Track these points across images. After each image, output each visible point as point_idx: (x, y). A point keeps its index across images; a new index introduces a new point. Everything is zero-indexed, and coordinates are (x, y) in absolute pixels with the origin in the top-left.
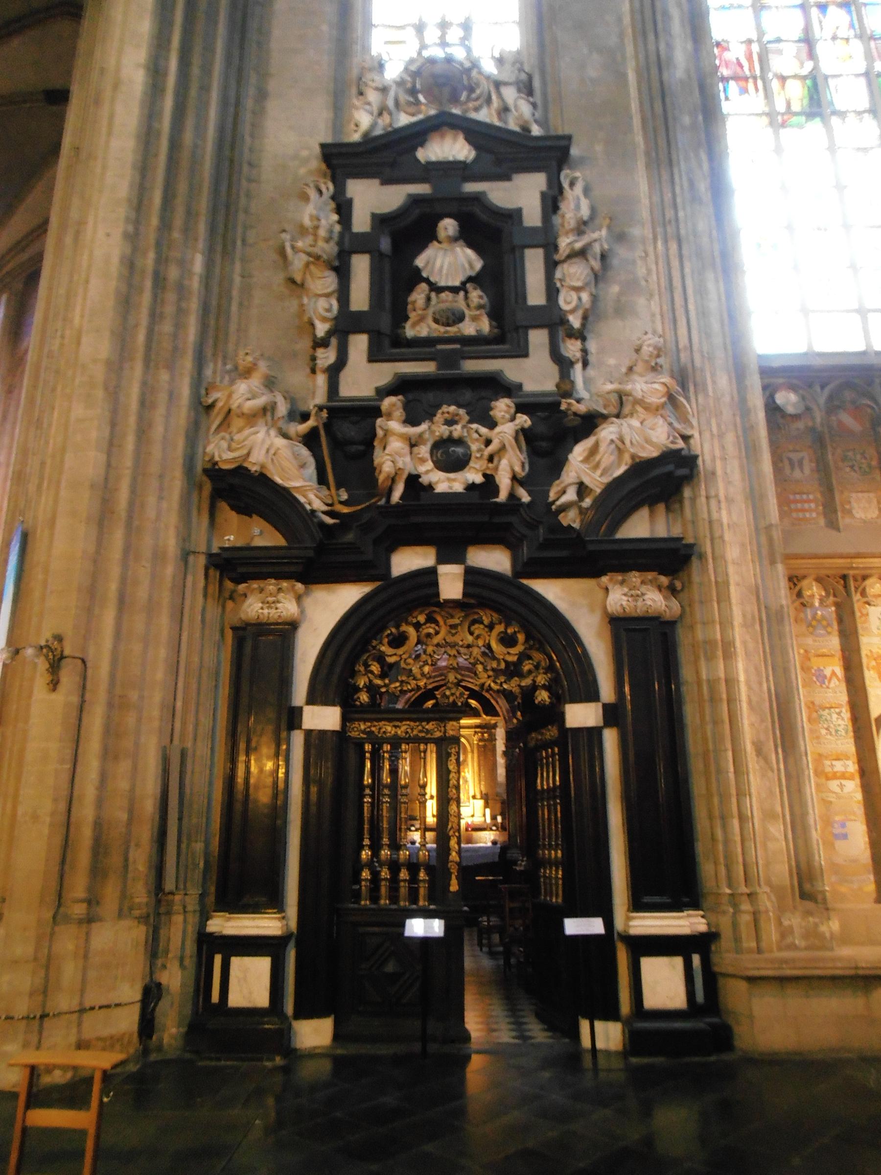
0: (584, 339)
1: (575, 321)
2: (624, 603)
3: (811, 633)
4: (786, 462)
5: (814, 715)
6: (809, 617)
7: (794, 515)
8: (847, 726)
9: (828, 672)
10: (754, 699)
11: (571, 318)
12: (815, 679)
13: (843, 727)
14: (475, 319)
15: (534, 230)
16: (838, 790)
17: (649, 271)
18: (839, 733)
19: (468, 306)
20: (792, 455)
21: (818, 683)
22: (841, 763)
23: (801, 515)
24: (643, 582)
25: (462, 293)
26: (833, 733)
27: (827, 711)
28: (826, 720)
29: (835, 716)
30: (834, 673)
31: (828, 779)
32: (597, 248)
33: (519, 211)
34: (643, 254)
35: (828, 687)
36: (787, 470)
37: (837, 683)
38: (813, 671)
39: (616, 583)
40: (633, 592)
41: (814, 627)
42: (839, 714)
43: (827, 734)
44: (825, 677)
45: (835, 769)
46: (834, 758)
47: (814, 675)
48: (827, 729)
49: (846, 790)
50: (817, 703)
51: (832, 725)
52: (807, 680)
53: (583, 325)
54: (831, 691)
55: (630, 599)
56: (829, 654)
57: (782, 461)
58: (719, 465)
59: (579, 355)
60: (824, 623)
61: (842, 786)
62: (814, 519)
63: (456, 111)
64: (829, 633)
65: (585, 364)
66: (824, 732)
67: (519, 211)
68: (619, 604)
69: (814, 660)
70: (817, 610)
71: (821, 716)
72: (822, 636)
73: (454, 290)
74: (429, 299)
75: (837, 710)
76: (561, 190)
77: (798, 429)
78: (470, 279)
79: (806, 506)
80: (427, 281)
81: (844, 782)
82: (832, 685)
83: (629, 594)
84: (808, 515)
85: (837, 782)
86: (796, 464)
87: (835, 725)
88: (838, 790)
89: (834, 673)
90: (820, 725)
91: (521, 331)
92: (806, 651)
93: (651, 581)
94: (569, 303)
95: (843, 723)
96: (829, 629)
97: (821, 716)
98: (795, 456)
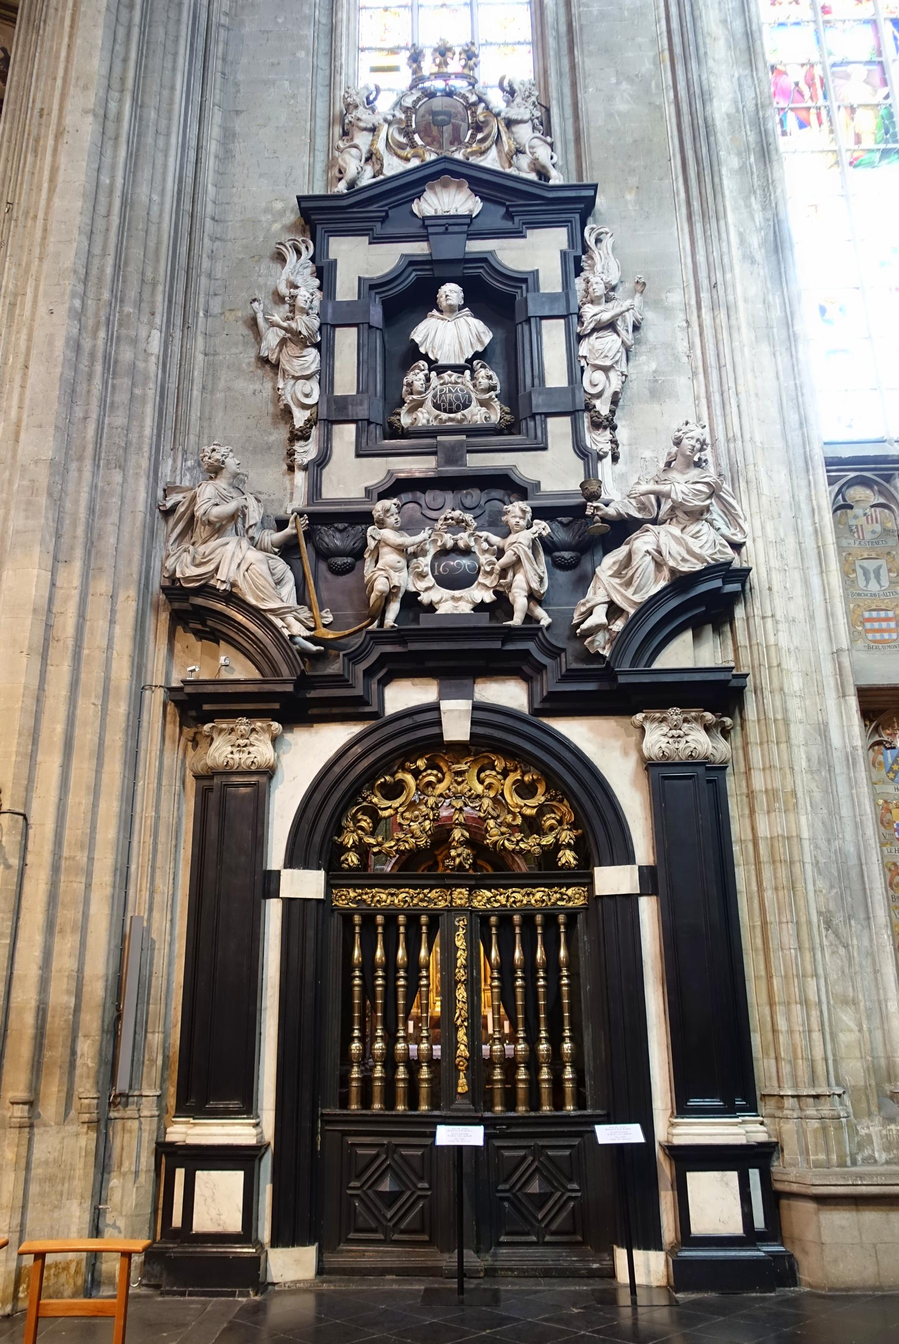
0: (614, 428)
1: (603, 407)
2: (663, 746)
3: (892, 780)
4: (860, 571)
6: (890, 761)
7: (870, 636)
10: (822, 860)
11: (597, 403)
14: (483, 403)
15: (552, 298)
17: (691, 347)
19: (475, 386)
20: (865, 563)
23: (878, 636)
24: (686, 720)
25: (467, 372)
32: (630, 318)
33: (535, 273)
34: (685, 324)
36: (861, 582)
39: (653, 720)
40: (674, 732)
53: (613, 412)
55: (671, 741)
57: (854, 571)
58: (776, 578)
59: (607, 447)
62: (894, 641)
63: (459, 156)
65: (615, 459)
67: (535, 273)
68: (658, 746)
73: (459, 369)
74: (428, 379)
76: (585, 249)
77: (873, 532)
78: (477, 355)
79: (884, 625)
80: (425, 357)
83: (670, 735)
84: (886, 636)
86: (872, 576)
91: (538, 417)
92: (886, 802)
93: (696, 719)
94: (596, 385)
98: (871, 565)
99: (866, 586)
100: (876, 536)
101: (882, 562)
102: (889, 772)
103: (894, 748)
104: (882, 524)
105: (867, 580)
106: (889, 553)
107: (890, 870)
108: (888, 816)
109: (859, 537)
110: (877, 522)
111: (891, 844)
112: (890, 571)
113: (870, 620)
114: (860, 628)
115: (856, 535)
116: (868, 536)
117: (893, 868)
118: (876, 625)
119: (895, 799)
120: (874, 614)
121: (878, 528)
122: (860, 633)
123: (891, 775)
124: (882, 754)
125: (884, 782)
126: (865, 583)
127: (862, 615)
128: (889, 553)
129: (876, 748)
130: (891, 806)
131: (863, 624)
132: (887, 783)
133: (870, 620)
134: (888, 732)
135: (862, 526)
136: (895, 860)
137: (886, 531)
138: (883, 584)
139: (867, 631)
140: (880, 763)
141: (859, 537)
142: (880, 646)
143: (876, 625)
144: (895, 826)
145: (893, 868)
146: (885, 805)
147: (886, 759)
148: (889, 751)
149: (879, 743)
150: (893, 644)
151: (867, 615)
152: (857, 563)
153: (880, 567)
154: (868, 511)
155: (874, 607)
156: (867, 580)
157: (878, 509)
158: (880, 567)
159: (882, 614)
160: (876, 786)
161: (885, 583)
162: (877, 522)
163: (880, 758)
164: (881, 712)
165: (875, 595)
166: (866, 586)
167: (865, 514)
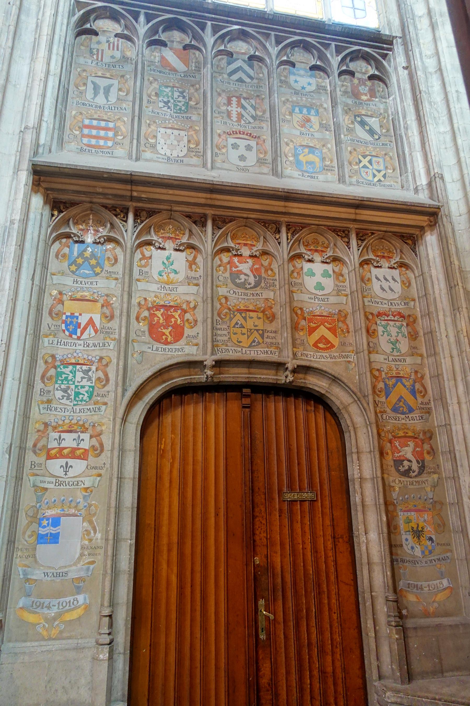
3: (73, 272)
4: (90, 86)
5: (52, 372)
6: (76, 254)
7: (85, 140)
8: (93, 387)
9: (83, 320)
12: (63, 326)
13: (87, 388)
16: (61, 472)
18: (81, 396)
20: (97, 80)
21: (67, 333)
22: (75, 435)
26: (72, 397)
27: (71, 367)
28: (66, 378)
29: (79, 375)
30: (91, 322)
31: (49, 457)
35: (79, 338)
36: (89, 94)
37: (93, 334)
38: (64, 317)
41: (79, 266)
42: (86, 372)
43: (63, 397)
44: (79, 325)
45: (63, 445)
46: (66, 428)
47: (64, 322)
48: (65, 391)
49: (70, 474)
50: (58, 357)
51: (73, 387)
52: (53, 328)
54: (82, 342)
56: (91, 298)
60: (93, 262)
61: (67, 467)
62: (109, 147)
64: (97, 274)
66: (59, 394)
69: (67, 303)
70: (88, 247)
71: (59, 374)
72: (87, 276)
75: (84, 367)
77: (112, 57)
81: (71, 462)
82: (85, 336)
85: (63, 462)
86: (102, 91)
87: (76, 386)
88: (61, 472)
89: (91, 322)
90: (57, 386)
92: (60, 293)
95: (89, 384)
96: (98, 270)
97: (59, 374)
99: (93, 99)
100: (114, 60)
101: (115, 82)
102: (71, 265)
103: (83, 242)
104: (123, 52)
105: (96, 93)
106: (123, 76)
107: (46, 362)
108: (59, 307)
109: (97, 59)
110: (118, 50)
111: (55, 336)
112: (120, 90)
113: (90, 127)
114: (77, 133)
115: (95, 57)
116: (107, 59)
117: (50, 360)
118: (94, 132)
119: (71, 291)
120: (95, 123)
121: (118, 55)
122: (76, 136)
123: (73, 268)
124: (69, 247)
125: (63, 274)
126: (93, 96)
127: (83, 122)
128: (123, 76)
129: (64, 240)
130: (65, 297)
131: (81, 129)
132: (67, 275)
133: (90, 127)
134: (81, 227)
135: (103, 50)
136: (54, 352)
137: (125, 59)
138: (109, 99)
139: (83, 136)
140: (64, 256)
141: (97, 59)
142: (93, 150)
143: (94, 132)
144: (64, 317)
145: (50, 360)
146: (59, 296)
147: (71, 252)
148: (76, 245)
149: (68, 236)
150: (107, 150)
151: (87, 122)
152: (90, 79)
153: (110, 86)
154: (112, 40)
155: (96, 116)
156: (96, 93)
157: (121, 40)
158: (110, 86)
159: (103, 124)
160: (54, 277)
161: (113, 98)
162: (118, 50)
163: (66, 250)
164: (73, 204)
165: (100, 107)
166: (93, 99)
167: (108, 41)
